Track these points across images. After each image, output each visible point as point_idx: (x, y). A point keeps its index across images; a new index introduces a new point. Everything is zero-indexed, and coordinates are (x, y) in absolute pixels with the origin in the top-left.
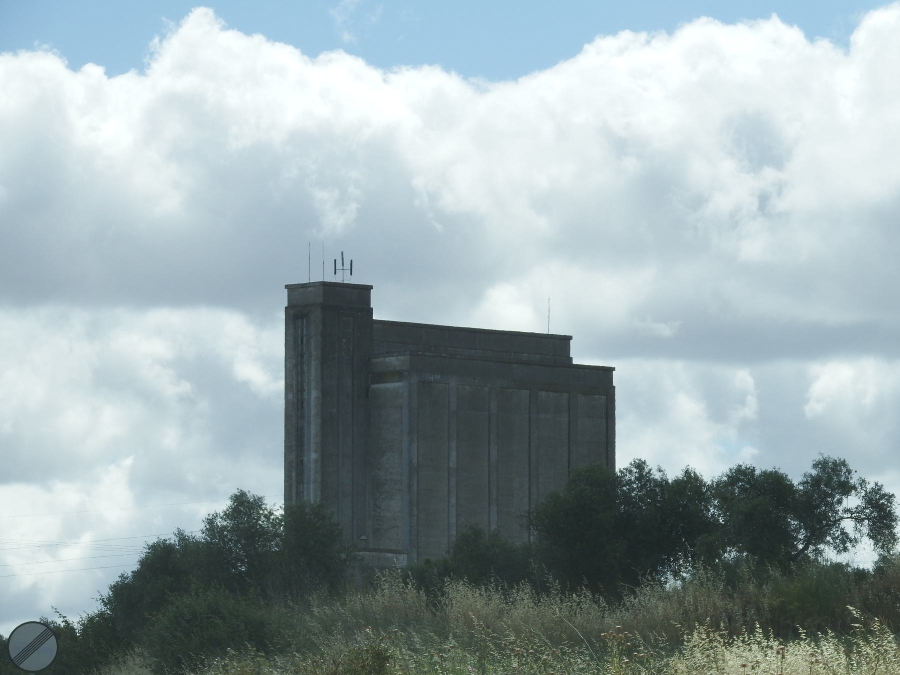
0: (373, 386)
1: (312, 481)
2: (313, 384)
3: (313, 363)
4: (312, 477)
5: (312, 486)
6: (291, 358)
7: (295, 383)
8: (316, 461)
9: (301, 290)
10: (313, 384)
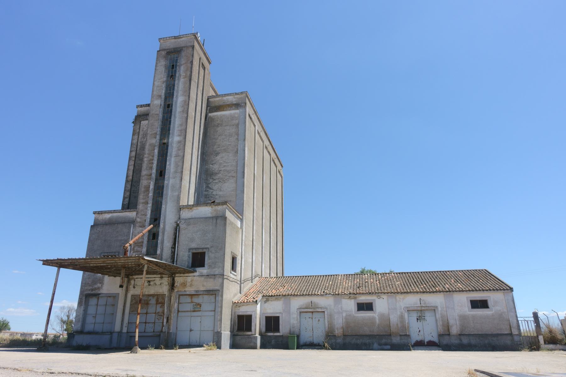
0: (210, 114)
1: (173, 155)
2: (180, 93)
3: (182, 80)
4: (174, 153)
5: (173, 159)
6: (159, 79)
7: (164, 92)
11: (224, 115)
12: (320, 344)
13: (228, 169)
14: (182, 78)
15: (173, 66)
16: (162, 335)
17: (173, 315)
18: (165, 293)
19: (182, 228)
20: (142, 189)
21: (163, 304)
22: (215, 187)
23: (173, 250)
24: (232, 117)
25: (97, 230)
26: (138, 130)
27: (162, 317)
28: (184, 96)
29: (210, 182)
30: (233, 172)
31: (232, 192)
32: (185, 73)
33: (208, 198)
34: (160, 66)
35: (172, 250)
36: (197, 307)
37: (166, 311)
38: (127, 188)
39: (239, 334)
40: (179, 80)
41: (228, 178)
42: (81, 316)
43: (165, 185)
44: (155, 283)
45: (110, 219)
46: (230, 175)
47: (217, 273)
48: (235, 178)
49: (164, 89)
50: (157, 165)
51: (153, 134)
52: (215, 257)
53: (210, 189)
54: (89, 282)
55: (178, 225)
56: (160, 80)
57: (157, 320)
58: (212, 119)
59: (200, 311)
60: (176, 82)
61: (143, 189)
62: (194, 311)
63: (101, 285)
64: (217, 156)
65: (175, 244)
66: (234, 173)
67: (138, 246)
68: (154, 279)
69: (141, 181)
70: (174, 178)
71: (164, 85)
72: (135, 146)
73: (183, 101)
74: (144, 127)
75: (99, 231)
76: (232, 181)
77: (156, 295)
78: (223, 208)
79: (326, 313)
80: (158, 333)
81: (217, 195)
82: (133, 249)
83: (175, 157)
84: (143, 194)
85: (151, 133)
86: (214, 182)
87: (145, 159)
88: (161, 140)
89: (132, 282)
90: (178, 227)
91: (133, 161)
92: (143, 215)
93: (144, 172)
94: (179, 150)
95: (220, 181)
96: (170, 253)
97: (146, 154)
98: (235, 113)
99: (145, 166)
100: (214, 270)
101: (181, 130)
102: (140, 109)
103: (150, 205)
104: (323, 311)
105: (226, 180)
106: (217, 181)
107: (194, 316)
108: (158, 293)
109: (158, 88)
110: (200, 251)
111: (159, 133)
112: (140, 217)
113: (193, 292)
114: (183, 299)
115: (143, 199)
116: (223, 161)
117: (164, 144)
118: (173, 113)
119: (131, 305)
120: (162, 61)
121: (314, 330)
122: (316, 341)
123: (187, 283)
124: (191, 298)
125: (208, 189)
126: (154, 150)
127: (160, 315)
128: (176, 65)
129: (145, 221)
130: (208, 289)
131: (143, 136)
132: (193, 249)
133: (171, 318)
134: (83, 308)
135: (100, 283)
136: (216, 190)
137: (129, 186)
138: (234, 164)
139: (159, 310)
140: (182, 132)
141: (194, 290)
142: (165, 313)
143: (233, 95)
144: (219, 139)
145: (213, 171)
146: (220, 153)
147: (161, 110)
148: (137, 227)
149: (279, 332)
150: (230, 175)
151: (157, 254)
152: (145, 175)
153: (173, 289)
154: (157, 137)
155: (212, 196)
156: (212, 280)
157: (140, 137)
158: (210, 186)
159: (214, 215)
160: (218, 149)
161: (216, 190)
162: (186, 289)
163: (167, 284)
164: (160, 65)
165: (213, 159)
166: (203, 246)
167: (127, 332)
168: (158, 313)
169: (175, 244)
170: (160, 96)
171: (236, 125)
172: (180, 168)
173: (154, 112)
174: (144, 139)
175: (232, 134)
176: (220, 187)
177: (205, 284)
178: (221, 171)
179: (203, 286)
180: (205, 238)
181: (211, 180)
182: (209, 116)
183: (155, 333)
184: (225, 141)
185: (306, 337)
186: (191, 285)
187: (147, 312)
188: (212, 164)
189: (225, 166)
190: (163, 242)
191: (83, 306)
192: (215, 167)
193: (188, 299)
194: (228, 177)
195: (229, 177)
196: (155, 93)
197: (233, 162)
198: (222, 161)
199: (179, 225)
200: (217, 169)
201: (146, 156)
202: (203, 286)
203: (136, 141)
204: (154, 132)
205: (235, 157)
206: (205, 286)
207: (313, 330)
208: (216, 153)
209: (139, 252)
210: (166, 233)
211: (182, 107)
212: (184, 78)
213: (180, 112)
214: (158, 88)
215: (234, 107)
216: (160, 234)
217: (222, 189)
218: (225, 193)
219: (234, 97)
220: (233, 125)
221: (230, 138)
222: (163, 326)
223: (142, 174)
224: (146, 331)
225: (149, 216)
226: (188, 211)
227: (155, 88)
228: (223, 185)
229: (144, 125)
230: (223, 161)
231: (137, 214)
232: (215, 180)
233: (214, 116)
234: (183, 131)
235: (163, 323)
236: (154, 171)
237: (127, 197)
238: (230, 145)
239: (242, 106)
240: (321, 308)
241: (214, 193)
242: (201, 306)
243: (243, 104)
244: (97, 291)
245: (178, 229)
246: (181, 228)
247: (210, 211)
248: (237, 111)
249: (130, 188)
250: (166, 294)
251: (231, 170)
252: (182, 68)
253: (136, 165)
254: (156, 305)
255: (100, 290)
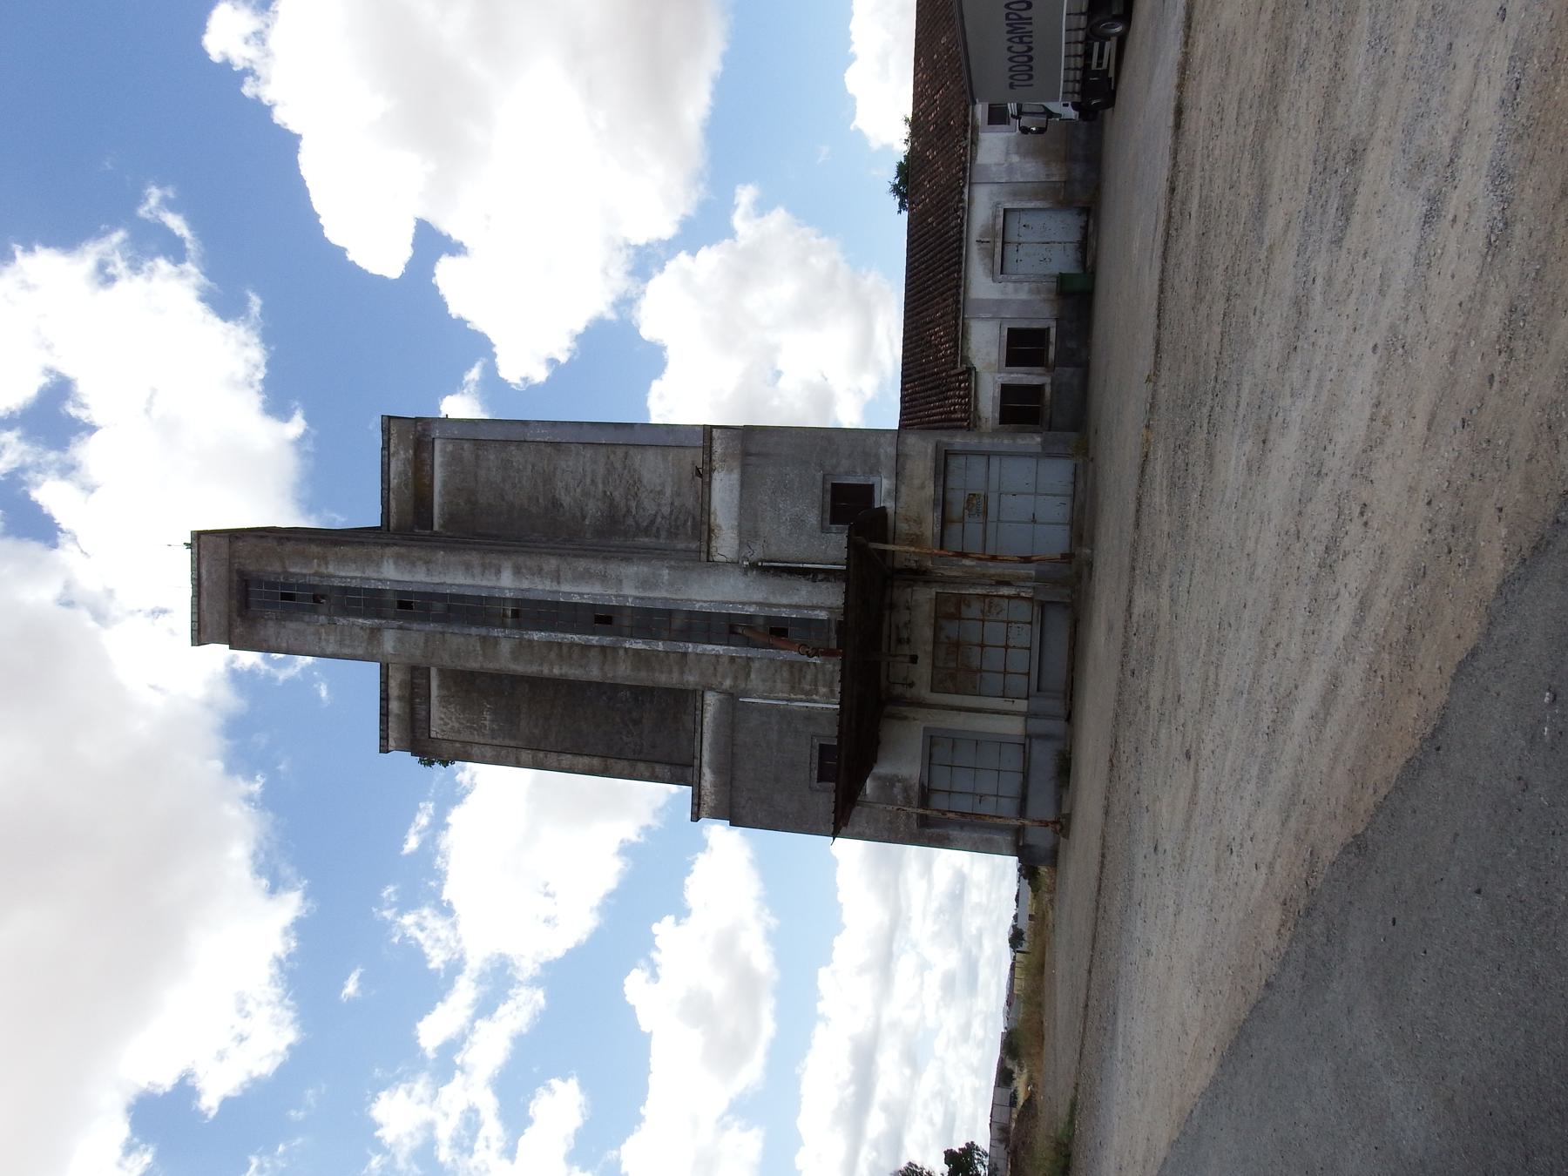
0: (436, 528)
1: (555, 587)
2: (370, 573)
3: (331, 569)
5: (565, 588)
6: (320, 639)
8: (517, 571)
9: (204, 603)
10: (370, 573)
11: (445, 484)
12: (1083, 224)
13: (601, 471)
14: (327, 568)
15: (286, 597)
16: (1042, 597)
17: (994, 569)
18: (934, 594)
19: (764, 552)
20: (643, 678)
21: (961, 600)
22: (650, 507)
23: (820, 577)
24: (454, 459)
25: (743, 807)
26: (458, 745)
27: (996, 599)
28: (382, 562)
29: (633, 523)
30: (612, 457)
31: (670, 458)
32: (313, 559)
33: (677, 527)
34: (279, 640)
35: (820, 581)
36: (977, 504)
37: (979, 591)
38: (624, 770)
39: (1048, 417)
40: (330, 576)
41: (629, 472)
42: (975, 835)
43: (638, 604)
44: (906, 624)
45: (717, 771)
46: (618, 465)
47: (892, 451)
48: (631, 452)
49: (351, 619)
50: (576, 633)
51: (484, 651)
52: (849, 455)
53: (653, 522)
54: (888, 819)
55: (753, 566)
56: (323, 637)
57: (1000, 617)
58: (451, 519)
59: (986, 497)
60: (335, 584)
61: (643, 674)
62: (986, 513)
63: (897, 784)
64: (561, 505)
65: (804, 573)
66: (614, 453)
67: (800, 680)
68: (893, 626)
69: (619, 681)
70: (621, 581)
71: (342, 621)
72: (504, 752)
73: (395, 563)
74: (449, 726)
75: (750, 799)
76: (637, 457)
77: (936, 621)
78: (718, 437)
79: (1008, 206)
80: (1036, 608)
81: (672, 504)
82: (806, 693)
83: (559, 583)
84: (657, 674)
85: (480, 658)
86: (634, 513)
87: (556, 671)
88: (504, 626)
89: (898, 690)
90: (760, 564)
91: (546, 757)
92: (715, 669)
93: (594, 673)
94: (541, 570)
95: (633, 493)
96: (829, 584)
97: (542, 671)
98: (443, 451)
99: (577, 672)
100: (882, 458)
101: (484, 567)
102: (392, 743)
103: (691, 647)
104: (1002, 213)
105: (632, 477)
106: (633, 504)
107: (999, 512)
108: (933, 615)
109: (347, 642)
110: (828, 497)
111: (483, 631)
112: (719, 680)
113: (935, 514)
114: (954, 544)
115: (671, 672)
116: (578, 486)
117: (516, 614)
118: (429, 590)
119: (957, 693)
120: (262, 633)
121: (1049, 240)
122: (1075, 236)
123: (911, 532)
124: (953, 522)
125: (654, 529)
126: (531, 641)
127: (990, 607)
128: (284, 585)
129: (732, 659)
130: (932, 474)
131: (475, 729)
132: (823, 520)
133: (999, 575)
134: (955, 833)
135: (893, 786)
136: (659, 505)
137: (621, 765)
138: (589, 453)
139: (974, 610)
140: (490, 563)
141: (931, 514)
142: (985, 592)
143: (389, 459)
144: (511, 498)
145: (602, 516)
146: (554, 496)
147: (415, 626)
148: (749, 687)
149: (1048, 329)
150: (618, 465)
151: (829, 620)
152: (602, 669)
153: (925, 571)
154: (496, 635)
155: (673, 517)
156: (909, 465)
157: (477, 739)
158: (645, 524)
159: (736, 464)
160: (540, 501)
161: (659, 505)
162: (928, 533)
163: (909, 590)
164: (277, 640)
165: (568, 514)
166: (818, 491)
167: (1027, 698)
168: (983, 612)
169: (804, 573)
170: (375, 633)
171: (478, 449)
172: (593, 566)
173: (418, 652)
174: (486, 726)
175: (502, 460)
176: (652, 495)
177: (917, 482)
178: (605, 492)
179: (922, 487)
180: (795, 487)
181: (630, 521)
182: (441, 530)
183: (1034, 621)
184: (520, 482)
185: (1063, 261)
186: (919, 521)
187: (978, 645)
188: (584, 518)
189: (593, 481)
190: (797, 607)
191: (951, 832)
192: (593, 508)
193: (955, 529)
194: (626, 471)
195: (625, 469)
196: (360, 651)
197: (584, 457)
198: (578, 490)
199: (754, 563)
200: (599, 503)
201: (546, 671)
202: (922, 487)
203: (490, 750)
204: (479, 648)
205: (571, 451)
206: (923, 483)
207: (1048, 243)
208: (554, 506)
209: (816, 677)
210: (772, 600)
211: (413, 564)
212: (327, 564)
213: (428, 570)
214: (347, 642)
215: (425, 455)
216: (774, 612)
217: (659, 488)
218: (669, 479)
219: (393, 455)
220: (477, 456)
221: (512, 466)
222: (1017, 597)
223: (598, 680)
224: (1029, 646)
225: (720, 649)
226: (717, 537)
227: (347, 651)
228: (645, 487)
229: (444, 728)
230: (578, 486)
231: (711, 689)
232: (629, 511)
233: (442, 515)
234: (487, 561)
235: (1009, 597)
236: (594, 640)
237: (650, 769)
238: (533, 466)
239: (424, 430)
240: (995, 217)
241: (666, 510)
242: (974, 495)
243: (419, 428)
244: (912, 794)
245: (765, 564)
246: (761, 556)
247: (722, 474)
248: (438, 445)
249: (626, 763)
250: (937, 593)
251: (606, 464)
252: (293, 570)
253: (559, 749)
254: (964, 619)
255: (911, 787)
